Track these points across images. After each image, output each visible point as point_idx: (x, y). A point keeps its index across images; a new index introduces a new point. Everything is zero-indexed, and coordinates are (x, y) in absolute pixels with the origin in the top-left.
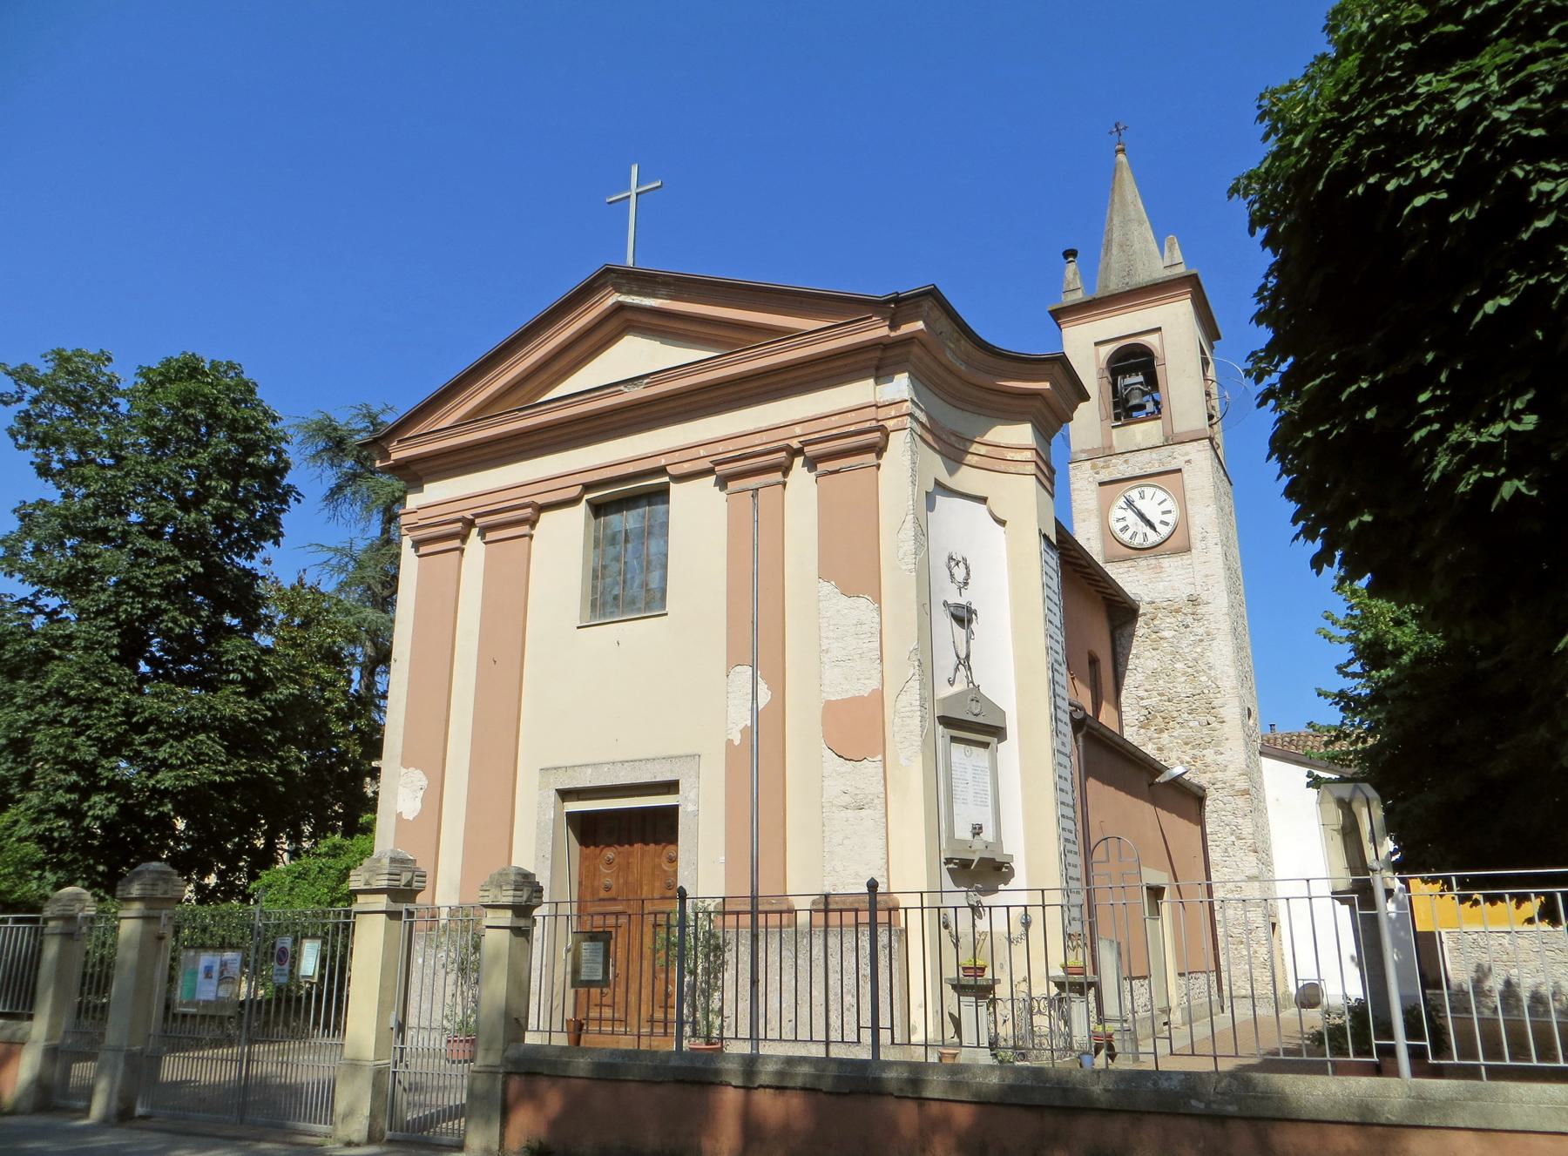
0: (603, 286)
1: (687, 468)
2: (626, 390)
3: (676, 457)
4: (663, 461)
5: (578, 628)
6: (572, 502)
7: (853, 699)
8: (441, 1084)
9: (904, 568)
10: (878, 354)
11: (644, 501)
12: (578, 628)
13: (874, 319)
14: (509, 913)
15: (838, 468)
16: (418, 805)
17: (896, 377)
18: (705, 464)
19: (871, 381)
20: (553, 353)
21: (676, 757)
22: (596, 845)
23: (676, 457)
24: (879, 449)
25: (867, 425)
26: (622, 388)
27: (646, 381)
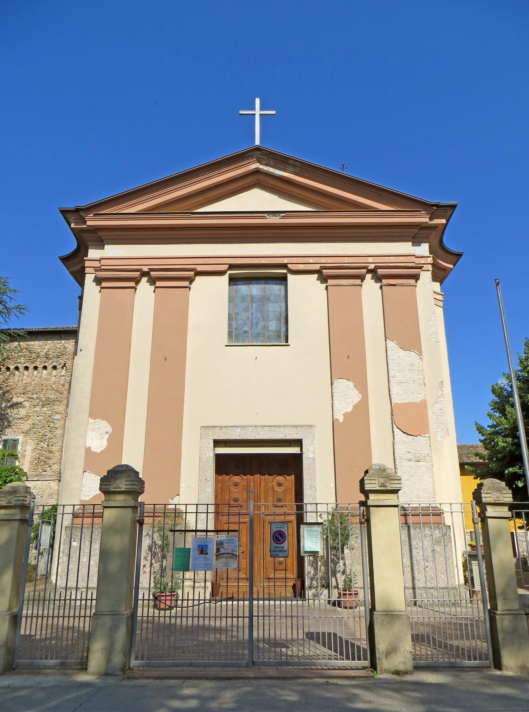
0: (251, 157)
1: (301, 267)
2: (268, 217)
3: (294, 260)
4: (286, 261)
5: (226, 346)
6: (221, 273)
7: (410, 404)
8: (71, 624)
9: (433, 340)
10: (416, 231)
11: (264, 282)
12: (226, 346)
13: (422, 212)
14: (506, 509)
15: (395, 283)
16: (105, 443)
17: (422, 244)
18: (317, 267)
19: (410, 243)
20: (212, 186)
21: (299, 426)
22: (227, 474)
23: (294, 260)
24: (416, 277)
25: (411, 265)
26: (266, 215)
27: (282, 215)
